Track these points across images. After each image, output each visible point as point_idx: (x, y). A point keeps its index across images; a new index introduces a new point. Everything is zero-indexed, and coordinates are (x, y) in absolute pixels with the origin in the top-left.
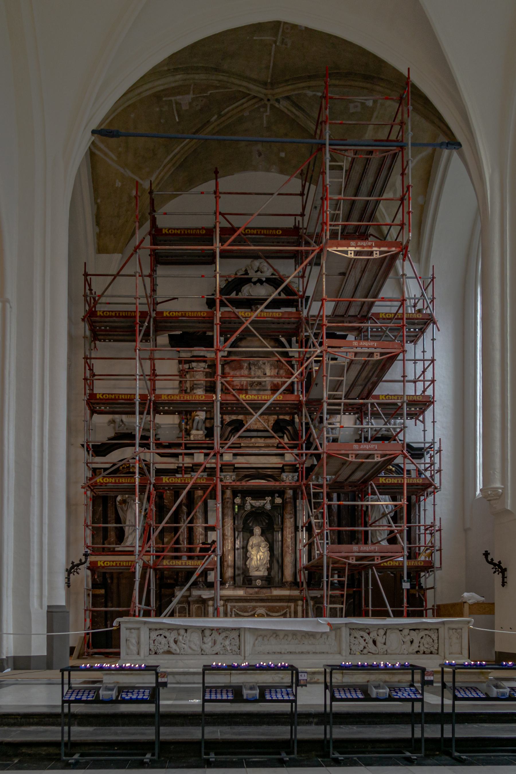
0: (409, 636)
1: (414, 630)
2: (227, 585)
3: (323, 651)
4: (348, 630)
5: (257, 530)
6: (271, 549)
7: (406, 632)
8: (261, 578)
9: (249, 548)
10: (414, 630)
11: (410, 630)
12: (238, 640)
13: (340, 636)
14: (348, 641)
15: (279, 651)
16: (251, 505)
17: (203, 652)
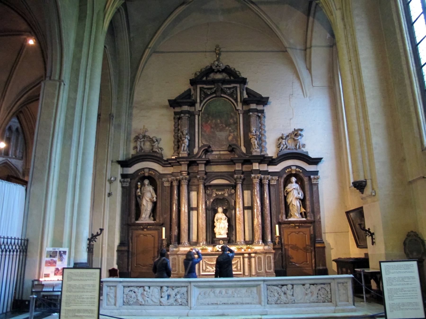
0: (310, 289)
1: (313, 284)
2: (202, 244)
3: (247, 302)
4: (266, 286)
5: (220, 210)
6: (229, 221)
7: (307, 286)
8: (223, 239)
9: (215, 220)
10: (313, 284)
11: (310, 284)
12: (186, 295)
13: (260, 291)
14: (266, 294)
15: (216, 303)
16: (216, 194)
17: (161, 304)
